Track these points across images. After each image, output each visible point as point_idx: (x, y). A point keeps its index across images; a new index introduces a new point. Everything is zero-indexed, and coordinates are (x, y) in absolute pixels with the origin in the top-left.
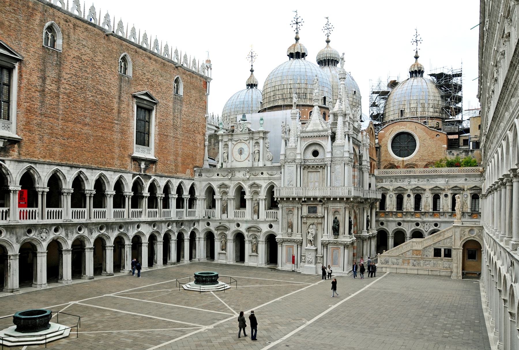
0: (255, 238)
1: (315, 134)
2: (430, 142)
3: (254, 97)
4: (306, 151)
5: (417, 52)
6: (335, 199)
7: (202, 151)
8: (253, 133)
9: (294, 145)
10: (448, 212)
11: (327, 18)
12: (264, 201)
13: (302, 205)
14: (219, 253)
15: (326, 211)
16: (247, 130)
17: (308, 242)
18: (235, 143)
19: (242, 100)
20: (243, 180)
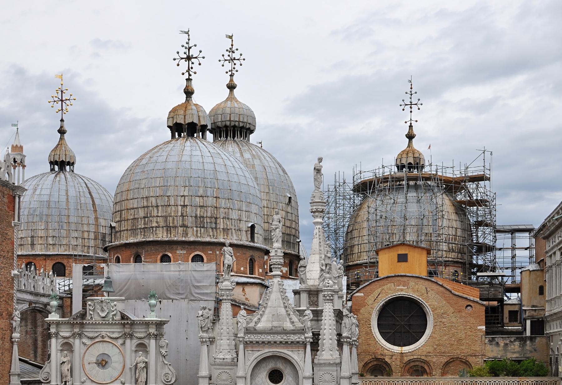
1: (278, 338)
2: (454, 320)
3: (72, 193)
4: (256, 371)
5: (411, 126)
7: (7, 354)
8: (133, 324)
9: (229, 357)
11: (231, 37)
16: (118, 317)
19: (46, 198)
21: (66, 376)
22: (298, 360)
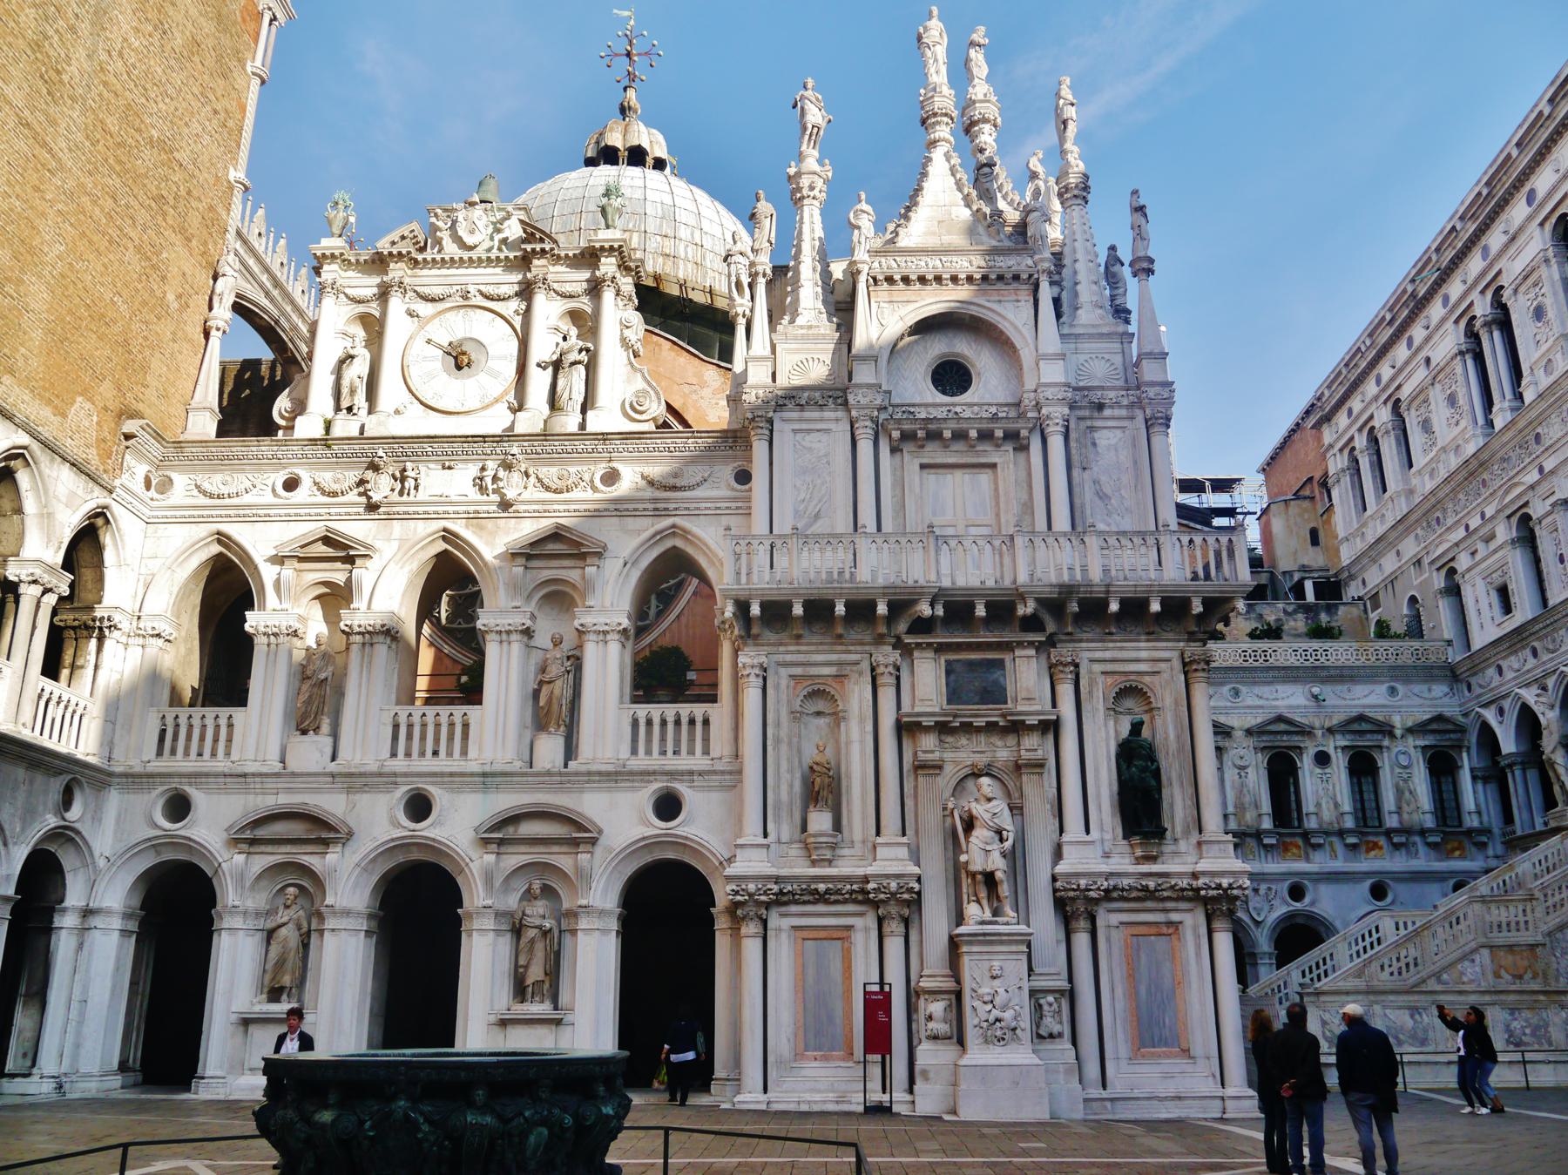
0: (548, 892)
6: (1134, 610)
10: (1341, 833)
12: (614, 647)
13: (907, 651)
14: (246, 1022)
15: (1066, 691)
17: (966, 883)
18: (425, 309)
20: (474, 518)
21: (353, 392)
22: (1020, 326)
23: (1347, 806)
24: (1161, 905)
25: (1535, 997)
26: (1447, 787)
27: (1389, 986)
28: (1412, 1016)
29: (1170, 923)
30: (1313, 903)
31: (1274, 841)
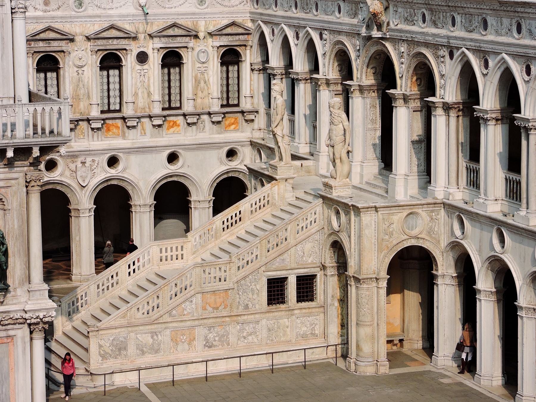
23: (157, 96)
24: (4, 328)
25: (223, 319)
26: (233, 73)
27: (141, 321)
28: (152, 337)
29: (8, 337)
30: (124, 170)
31: (99, 125)
